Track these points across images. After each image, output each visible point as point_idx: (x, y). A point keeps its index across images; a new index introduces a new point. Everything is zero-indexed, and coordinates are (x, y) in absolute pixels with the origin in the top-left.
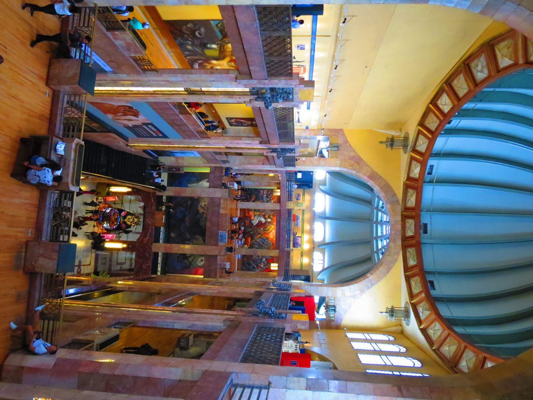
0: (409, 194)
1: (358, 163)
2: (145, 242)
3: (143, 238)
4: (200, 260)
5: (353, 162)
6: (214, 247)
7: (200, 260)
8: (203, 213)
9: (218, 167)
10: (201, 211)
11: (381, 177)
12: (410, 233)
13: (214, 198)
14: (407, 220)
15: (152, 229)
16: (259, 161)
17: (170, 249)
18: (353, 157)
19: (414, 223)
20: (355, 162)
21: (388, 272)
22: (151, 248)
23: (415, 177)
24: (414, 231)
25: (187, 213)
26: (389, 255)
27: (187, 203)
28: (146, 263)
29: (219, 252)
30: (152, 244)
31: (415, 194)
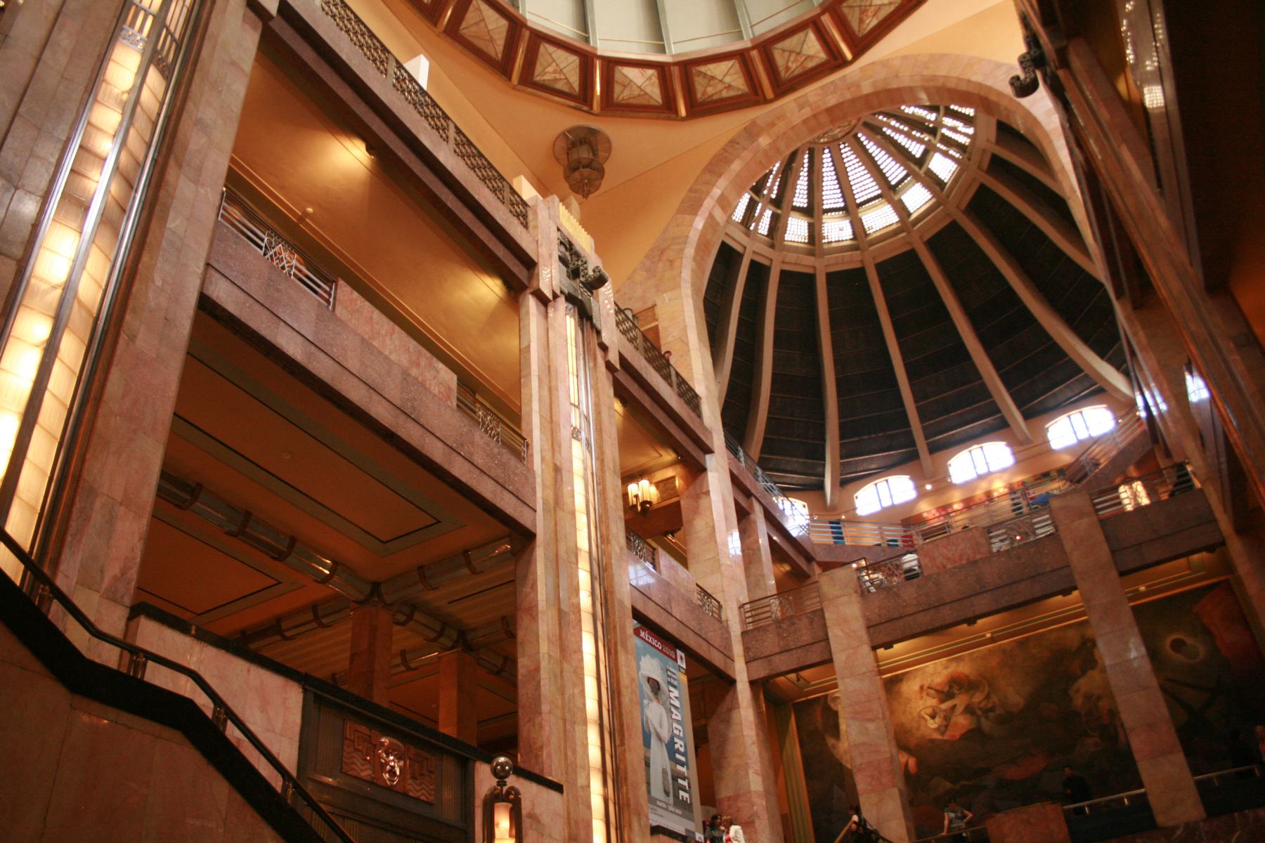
0: (710, 90)
1: (662, 252)
4: (1179, 658)
5: (661, 265)
6: (1068, 546)
7: (1179, 658)
8: (969, 710)
9: (747, 649)
10: (962, 722)
11: (690, 190)
12: (812, 47)
13: (867, 619)
14: (784, 74)
18: (648, 270)
19: (780, 45)
20: (660, 260)
21: (946, 55)
22: (1191, 828)
23: (655, 80)
24: (801, 35)
26: (897, 76)
31: (703, 69)
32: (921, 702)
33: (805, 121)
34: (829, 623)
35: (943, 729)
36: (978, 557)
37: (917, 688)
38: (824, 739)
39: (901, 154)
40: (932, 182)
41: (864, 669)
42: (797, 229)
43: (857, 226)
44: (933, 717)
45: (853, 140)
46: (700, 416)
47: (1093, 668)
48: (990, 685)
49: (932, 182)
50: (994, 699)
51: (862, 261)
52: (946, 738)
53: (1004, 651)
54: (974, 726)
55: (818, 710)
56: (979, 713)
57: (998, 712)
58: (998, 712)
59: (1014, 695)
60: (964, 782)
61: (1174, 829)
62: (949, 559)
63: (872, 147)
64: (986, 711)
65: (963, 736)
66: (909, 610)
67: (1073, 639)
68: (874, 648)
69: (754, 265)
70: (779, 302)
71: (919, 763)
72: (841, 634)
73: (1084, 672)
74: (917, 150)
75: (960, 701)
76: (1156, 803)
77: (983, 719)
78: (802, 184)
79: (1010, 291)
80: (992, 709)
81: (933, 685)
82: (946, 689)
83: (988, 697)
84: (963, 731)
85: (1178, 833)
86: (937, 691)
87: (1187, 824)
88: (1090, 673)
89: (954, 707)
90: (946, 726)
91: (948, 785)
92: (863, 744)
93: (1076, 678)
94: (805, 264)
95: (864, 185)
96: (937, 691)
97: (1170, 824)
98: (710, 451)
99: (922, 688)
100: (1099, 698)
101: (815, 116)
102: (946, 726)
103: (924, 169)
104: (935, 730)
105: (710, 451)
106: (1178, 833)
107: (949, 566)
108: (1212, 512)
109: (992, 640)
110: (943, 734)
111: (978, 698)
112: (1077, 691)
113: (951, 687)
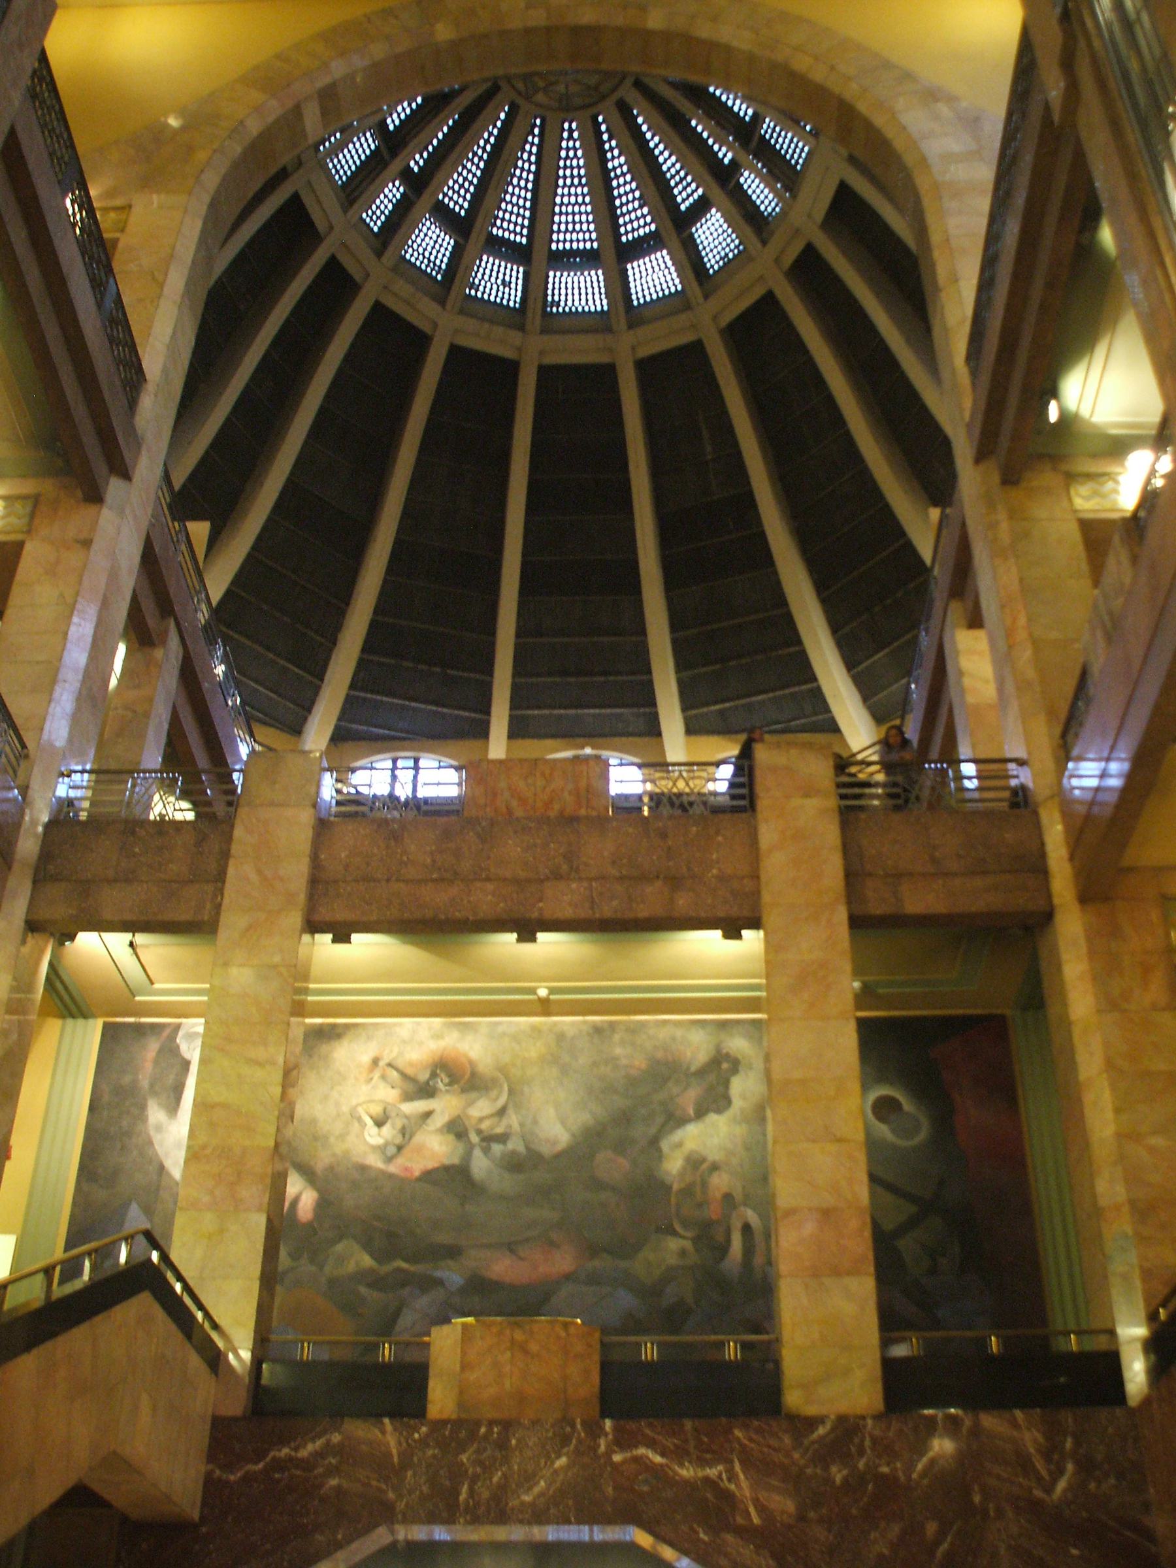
2: (784, 1505)
3: (746, 1532)
8: (457, 1129)
10: (435, 1148)
15: (623, 1441)
16: (52, 571)
17: (826, 1214)
22: (848, 1427)
25: (453, 1275)
27: (362, 1276)
28: (1024, 1464)
29: (808, 792)
30: (804, 1424)
32: (365, 1089)
33: (528, 31)
34: (235, 848)
35: (392, 1150)
36: (583, 812)
37: (366, 1059)
38: (143, 1108)
39: (657, 187)
40: (690, 258)
41: (277, 959)
42: (430, 244)
43: (534, 287)
44: (379, 1124)
45: (589, 123)
46: (132, 404)
47: (719, 1111)
48: (511, 1092)
49: (690, 258)
50: (513, 1120)
51: (519, 349)
52: (392, 1169)
53: (561, 1037)
54: (456, 1160)
55: (153, 1047)
56: (474, 1138)
57: (510, 1146)
58: (510, 1146)
59: (554, 1119)
60: (404, 1265)
61: (812, 1423)
62: (523, 801)
63: (617, 162)
64: (489, 1139)
65: (429, 1176)
66: (412, 872)
67: (696, 1046)
68: (313, 927)
69: (333, 266)
70: (349, 358)
71: (323, 1205)
72: (254, 877)
73: (700, 1114)
74: (686, 194)
75: (445, 1106)
76: (793, 1365)
77: (477, 1153)
78: (470, 170)
79: (748, 501)
80: (503, 1138)
81: (400, 1063)
82: (424, 1076)
83: (502, 1112)
84: (431, 1165)
85: (821, 1431)
86: (404, 1076)
87: (842, 1419)
88: (712, 1117)
89: (428, 1115)
90: (400, 1148)
91: (367, 1261)
92: (225, 1106)
93: (683, 1121)
94: (420, 311)
95: (575, 227)
96: (404, 1076)
97: (811, 1410)
98: (126, 476)
99: (375, 1062)
100: (715, 1167)
101: (548, 30)
102: (400, 1148)
103: (685, 234)
104: (375, 1148)
105: (126, 476)
106: (821, 1431)
107: (519, 813)
108: (1043, 855)
109: (545, 1007)
110: (389, 1160)
111: (481, 1109)
112: (680, 1145)
113: (434, 1075)
